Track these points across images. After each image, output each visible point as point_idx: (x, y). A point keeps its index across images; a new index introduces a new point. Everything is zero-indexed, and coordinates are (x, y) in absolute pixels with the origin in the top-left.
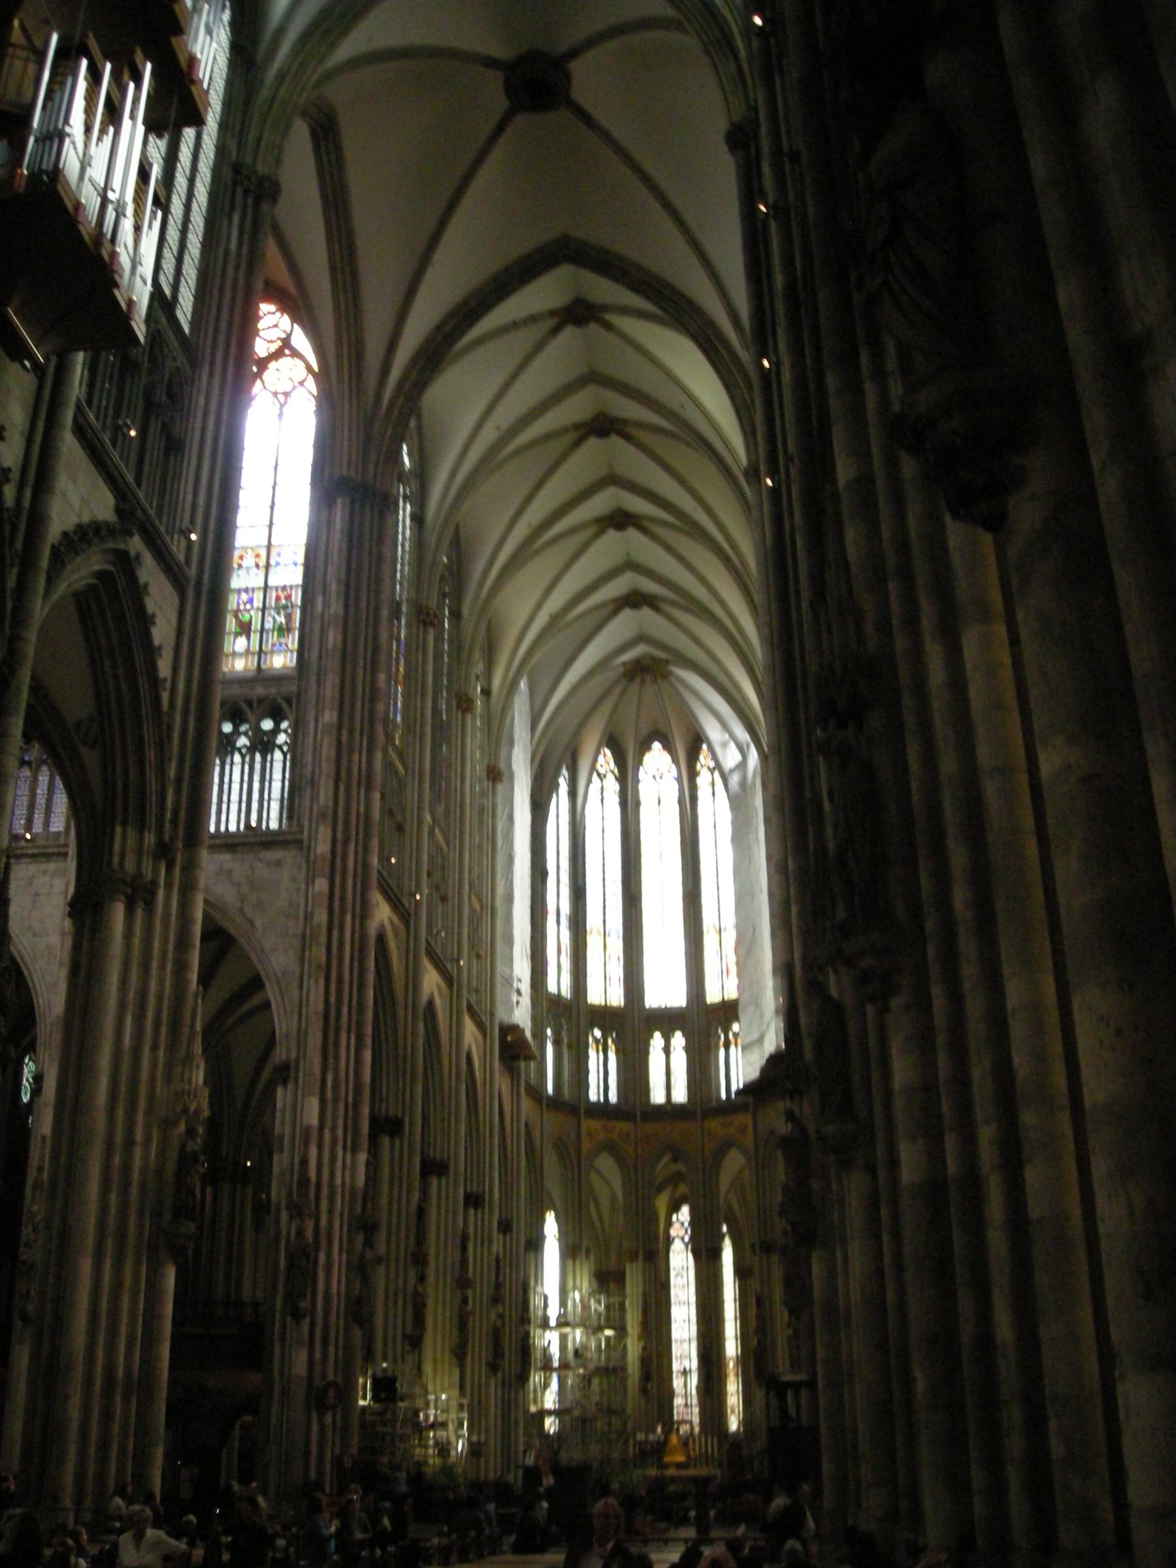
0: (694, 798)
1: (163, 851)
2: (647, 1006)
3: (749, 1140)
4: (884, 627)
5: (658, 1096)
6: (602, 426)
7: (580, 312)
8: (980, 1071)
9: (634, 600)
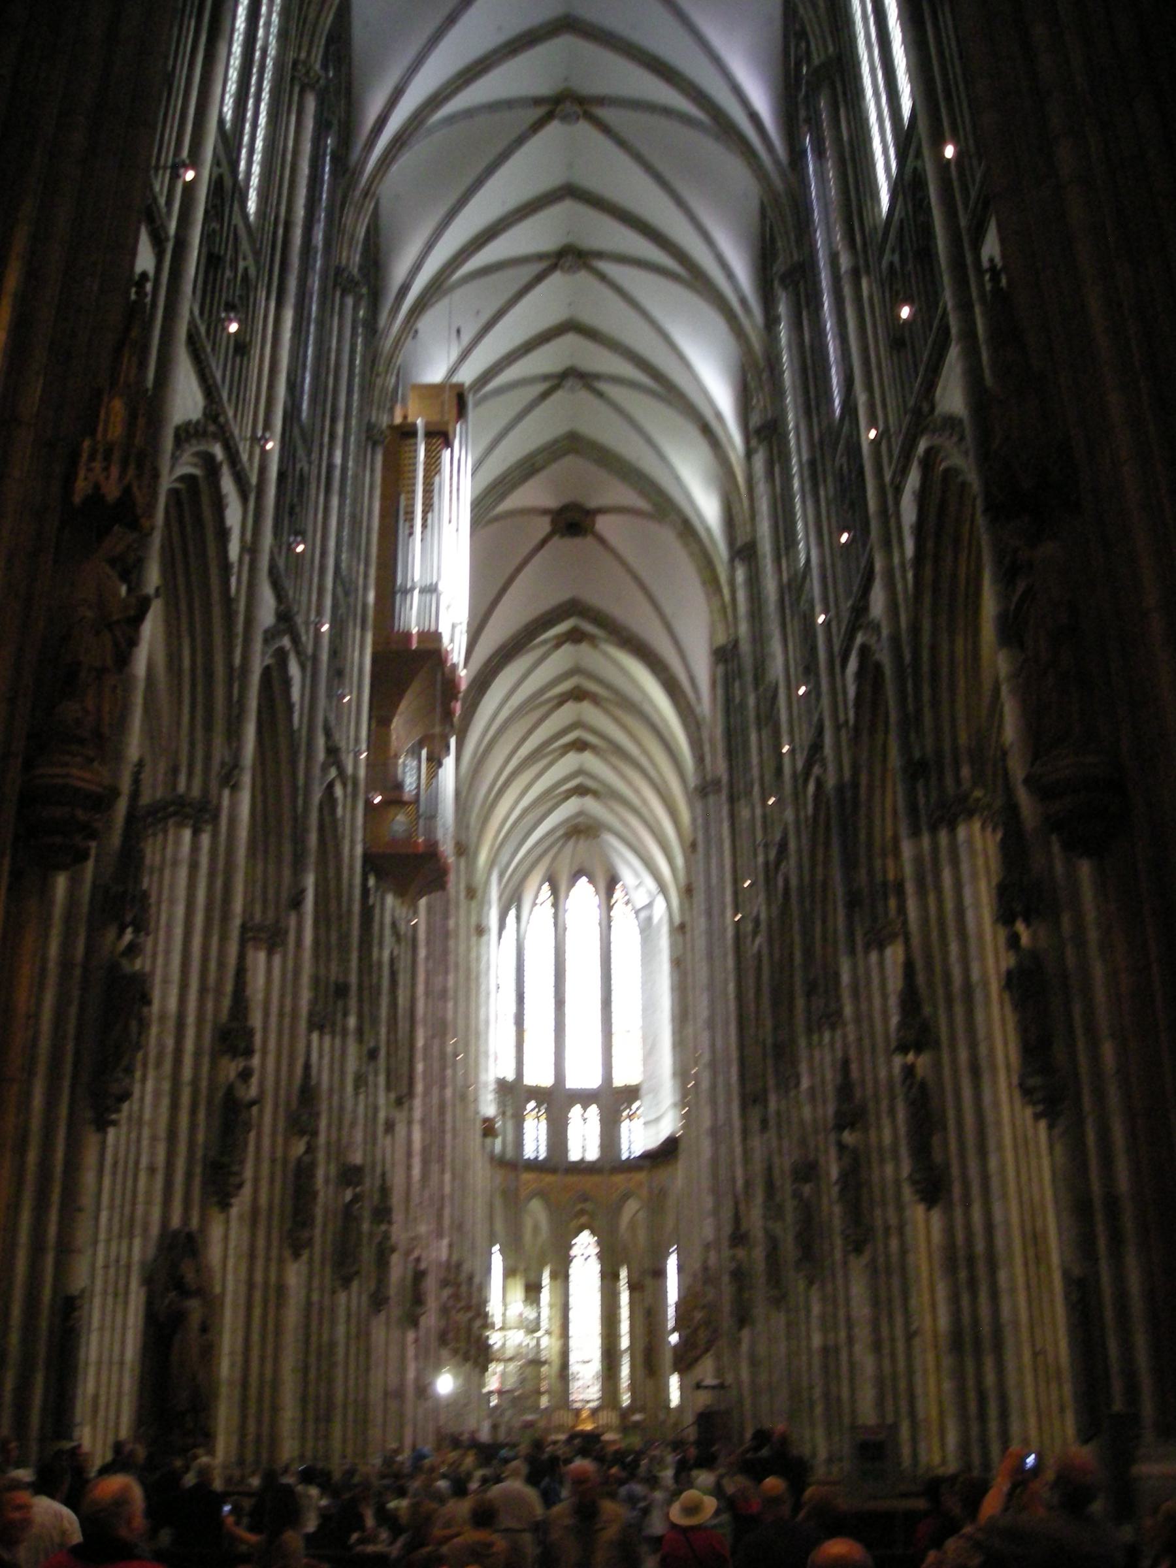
0: (610, 927)
1: (399, 1102)
2: (567, 1087)
3: (644, 1192)
4: (817, 1149)
5: (574, 1155)
6: (578, 695)
7: (575, 637)
8: (841, 1314)
9: (581, 791)
